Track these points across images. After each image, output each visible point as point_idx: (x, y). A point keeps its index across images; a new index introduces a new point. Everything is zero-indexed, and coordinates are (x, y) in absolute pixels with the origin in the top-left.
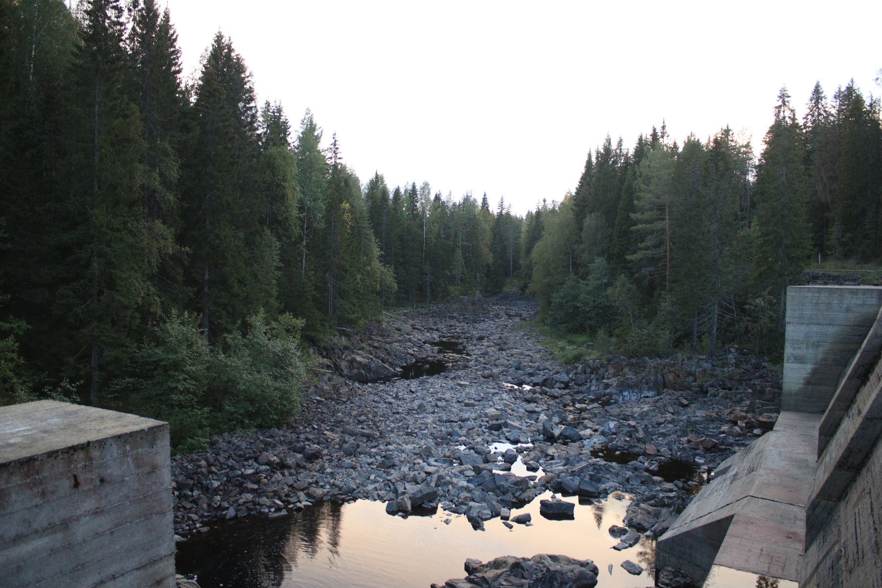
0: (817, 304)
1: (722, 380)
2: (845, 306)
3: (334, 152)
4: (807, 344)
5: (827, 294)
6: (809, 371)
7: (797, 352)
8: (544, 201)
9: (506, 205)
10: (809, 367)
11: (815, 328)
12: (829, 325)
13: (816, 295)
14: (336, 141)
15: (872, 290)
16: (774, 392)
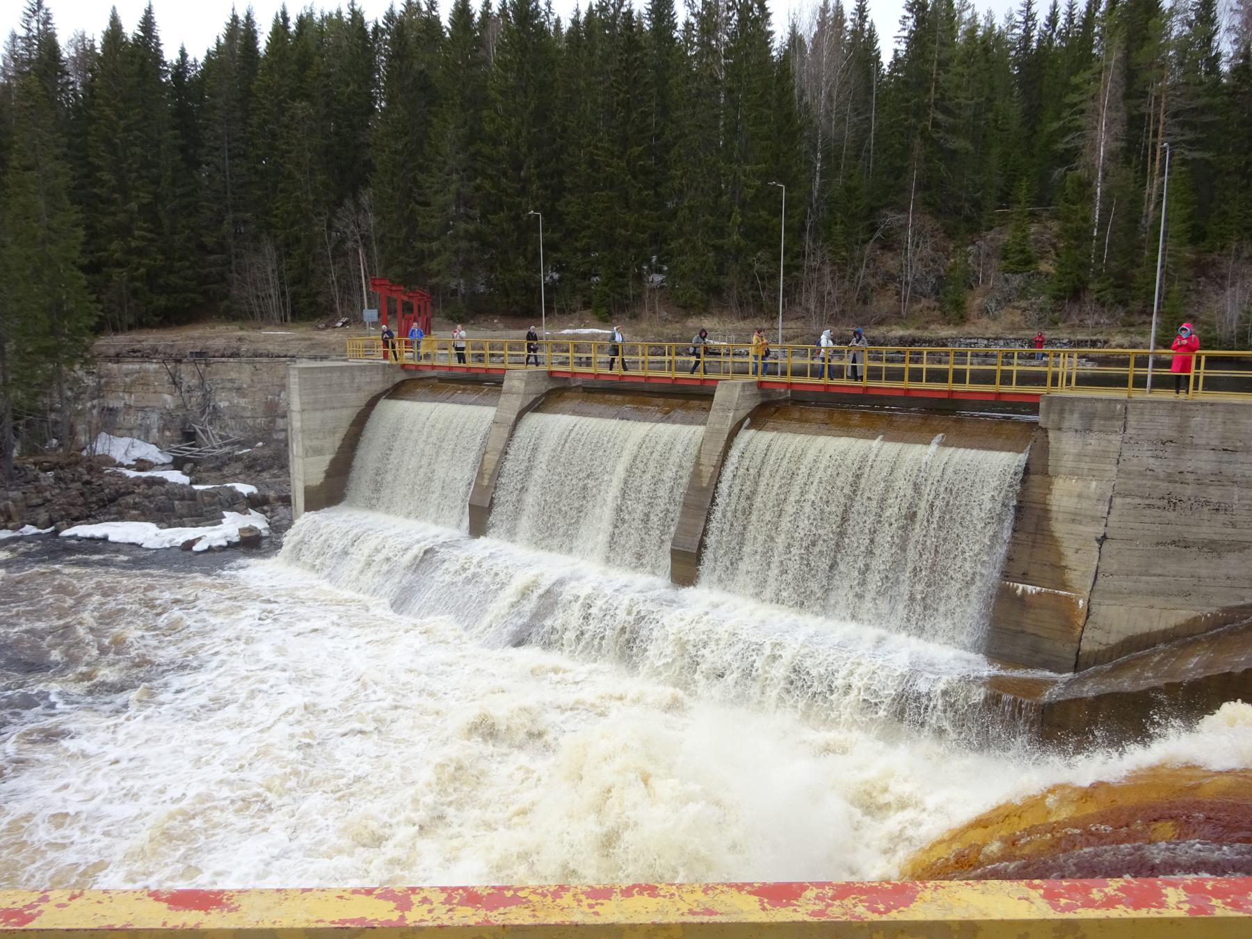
0: (330, 385)
1: (63, 509)
2: (356, 385)
5: (339, 374)
6: (328, 462)
10: (327, 458)
11: (330, 413)
12: (343, 407)
13: (329, 375)
15: (342, 367)
16: (189, 505)
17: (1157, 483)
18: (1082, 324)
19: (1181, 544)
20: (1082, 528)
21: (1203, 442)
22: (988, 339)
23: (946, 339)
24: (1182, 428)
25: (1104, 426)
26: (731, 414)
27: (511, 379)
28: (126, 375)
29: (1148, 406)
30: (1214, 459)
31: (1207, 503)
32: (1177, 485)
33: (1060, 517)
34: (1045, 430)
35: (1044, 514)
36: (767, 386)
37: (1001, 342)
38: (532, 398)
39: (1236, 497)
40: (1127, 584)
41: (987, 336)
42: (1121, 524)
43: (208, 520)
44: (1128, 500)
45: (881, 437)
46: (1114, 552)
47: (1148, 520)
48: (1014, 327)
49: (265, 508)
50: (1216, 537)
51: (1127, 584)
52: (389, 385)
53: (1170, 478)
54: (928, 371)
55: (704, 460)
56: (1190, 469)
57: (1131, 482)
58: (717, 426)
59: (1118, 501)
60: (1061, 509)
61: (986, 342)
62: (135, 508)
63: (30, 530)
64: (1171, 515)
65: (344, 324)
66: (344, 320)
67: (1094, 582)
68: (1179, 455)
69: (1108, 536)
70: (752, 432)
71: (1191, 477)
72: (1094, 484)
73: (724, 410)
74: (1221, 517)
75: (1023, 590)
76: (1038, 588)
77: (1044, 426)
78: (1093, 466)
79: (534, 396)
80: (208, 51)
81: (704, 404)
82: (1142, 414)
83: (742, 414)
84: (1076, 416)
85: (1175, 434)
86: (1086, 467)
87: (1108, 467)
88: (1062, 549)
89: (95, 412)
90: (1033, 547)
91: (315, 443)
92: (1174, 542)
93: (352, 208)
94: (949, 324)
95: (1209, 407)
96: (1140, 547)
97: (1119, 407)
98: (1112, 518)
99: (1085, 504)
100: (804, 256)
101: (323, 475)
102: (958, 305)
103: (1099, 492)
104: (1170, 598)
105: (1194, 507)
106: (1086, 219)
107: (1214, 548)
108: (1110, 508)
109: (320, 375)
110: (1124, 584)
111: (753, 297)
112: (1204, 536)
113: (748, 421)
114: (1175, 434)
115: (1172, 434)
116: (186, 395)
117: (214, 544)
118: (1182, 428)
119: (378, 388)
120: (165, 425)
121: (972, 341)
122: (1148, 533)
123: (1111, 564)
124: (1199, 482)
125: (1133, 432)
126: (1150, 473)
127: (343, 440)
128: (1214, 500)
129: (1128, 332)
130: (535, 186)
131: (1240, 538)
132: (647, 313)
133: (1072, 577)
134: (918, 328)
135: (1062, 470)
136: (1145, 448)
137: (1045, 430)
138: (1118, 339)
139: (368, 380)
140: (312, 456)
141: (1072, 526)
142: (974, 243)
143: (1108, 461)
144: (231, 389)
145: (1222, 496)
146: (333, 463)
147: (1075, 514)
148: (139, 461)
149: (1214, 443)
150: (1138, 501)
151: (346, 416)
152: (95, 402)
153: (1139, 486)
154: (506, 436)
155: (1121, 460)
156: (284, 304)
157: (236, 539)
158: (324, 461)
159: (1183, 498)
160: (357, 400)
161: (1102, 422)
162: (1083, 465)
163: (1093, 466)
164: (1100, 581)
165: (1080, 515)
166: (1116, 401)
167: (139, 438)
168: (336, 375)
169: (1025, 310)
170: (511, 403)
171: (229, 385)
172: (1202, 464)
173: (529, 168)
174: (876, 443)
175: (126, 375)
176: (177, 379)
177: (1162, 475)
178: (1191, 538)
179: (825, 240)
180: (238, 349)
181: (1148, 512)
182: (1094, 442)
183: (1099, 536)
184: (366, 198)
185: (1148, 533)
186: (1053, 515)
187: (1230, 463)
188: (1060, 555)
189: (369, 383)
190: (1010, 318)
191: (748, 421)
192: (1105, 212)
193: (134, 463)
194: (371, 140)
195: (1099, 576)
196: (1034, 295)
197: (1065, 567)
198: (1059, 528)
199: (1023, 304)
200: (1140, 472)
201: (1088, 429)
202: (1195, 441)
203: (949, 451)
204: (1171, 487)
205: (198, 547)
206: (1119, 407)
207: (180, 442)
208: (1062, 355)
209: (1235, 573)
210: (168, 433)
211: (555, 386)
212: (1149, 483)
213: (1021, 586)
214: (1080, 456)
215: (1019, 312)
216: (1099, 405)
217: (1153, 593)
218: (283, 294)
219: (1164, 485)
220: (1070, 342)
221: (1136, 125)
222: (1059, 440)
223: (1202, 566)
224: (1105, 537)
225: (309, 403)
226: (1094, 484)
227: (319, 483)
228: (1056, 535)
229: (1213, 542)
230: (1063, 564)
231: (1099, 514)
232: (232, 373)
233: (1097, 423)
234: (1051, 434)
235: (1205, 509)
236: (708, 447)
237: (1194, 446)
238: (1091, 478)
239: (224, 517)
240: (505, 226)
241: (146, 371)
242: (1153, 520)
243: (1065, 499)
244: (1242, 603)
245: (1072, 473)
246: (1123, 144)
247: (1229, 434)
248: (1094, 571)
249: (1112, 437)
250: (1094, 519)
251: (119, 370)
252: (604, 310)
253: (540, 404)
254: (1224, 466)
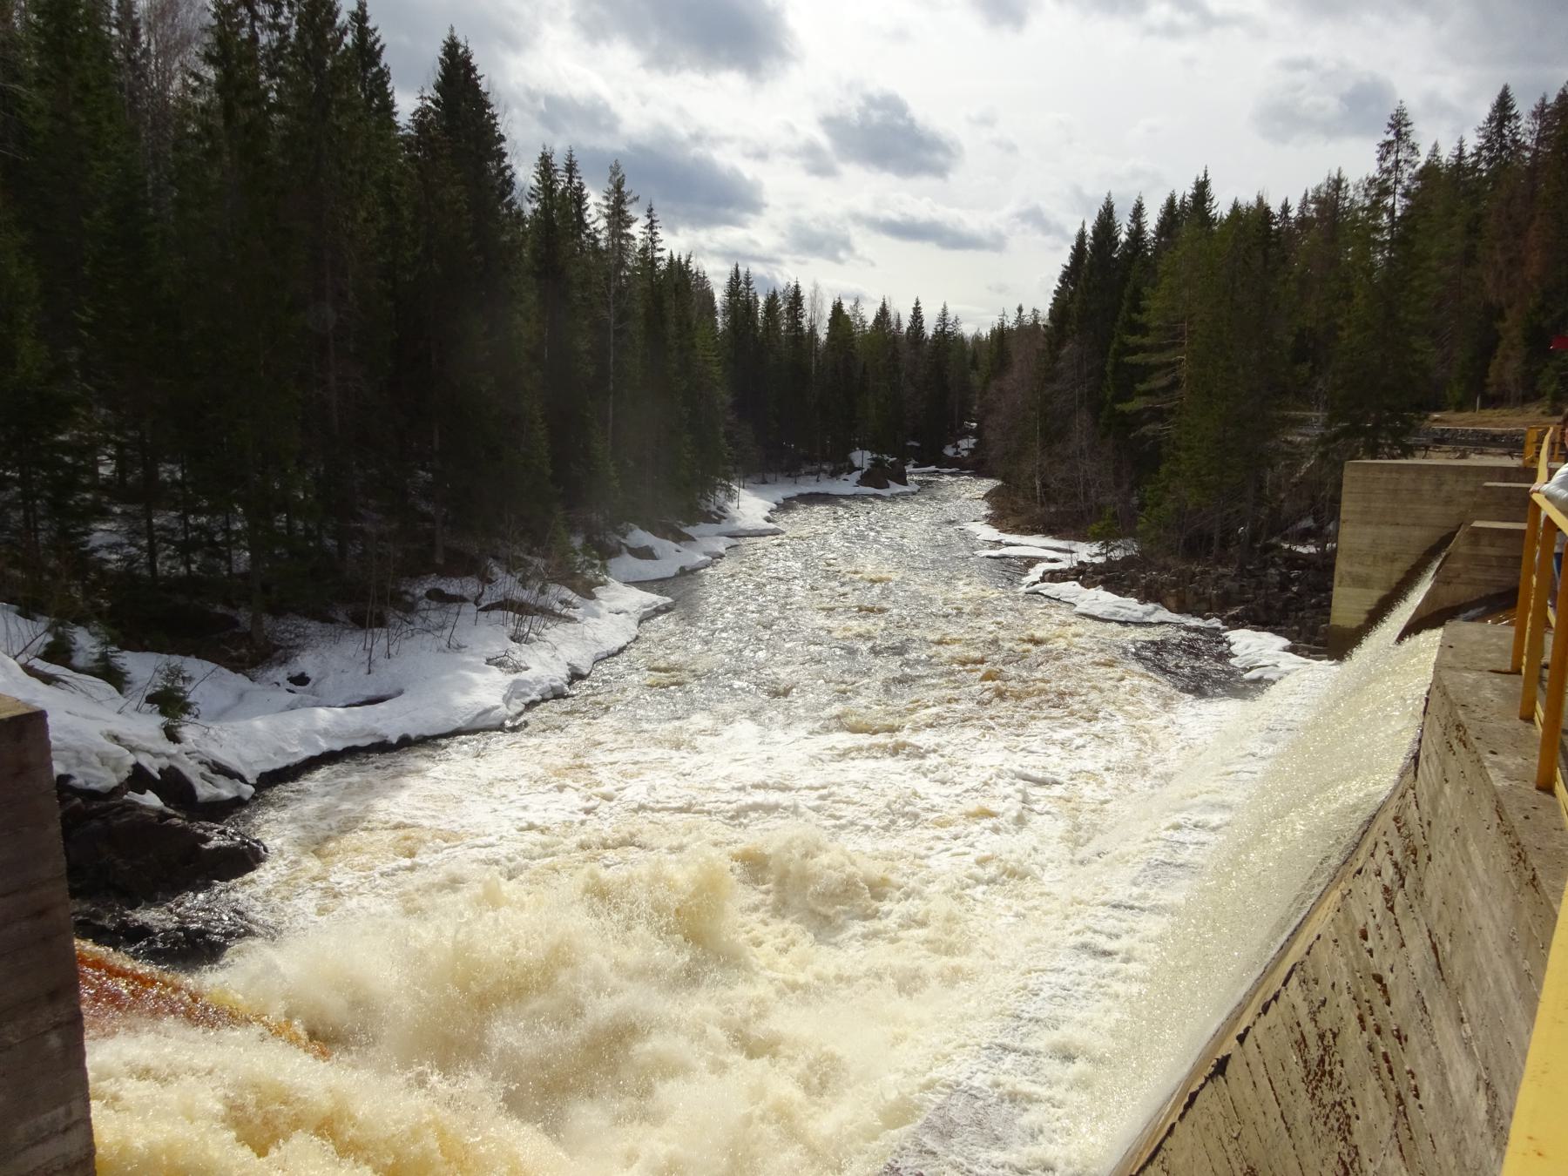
3: (651, 239)
4: (1375, 557)
6: (1375, 600)
7: (1358, 569)
8: (1020, 310)
9: (951, 317)
11: (1389, 531)
12: (1414, 525)
13: (1395, 475)
14: (652, 221)
63: (1215, 623)
101: (1364, 617)
139: (1470, 488)
140: (1349, 586)
191: (1472, 613)
195: (1159, 1158)
227: (1355, 625)
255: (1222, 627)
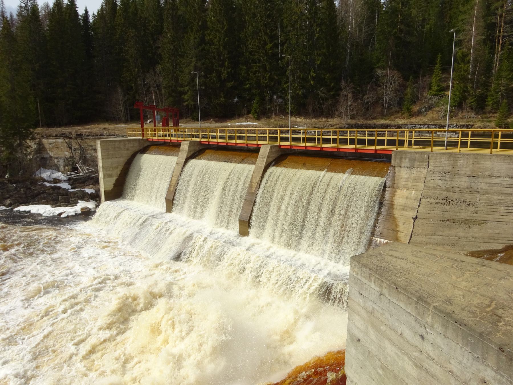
0: (115, 148)
2: (126, 148)
5: (118, 143)
6: (115, 180)
11: (115, 160)
13: (114, 143)
16: (65, 198)
17: (442, 192)
18: (463, 118)
19: (451, 221)
20: (407, 213)
21: (463, 172)
22: (420, 125)
23: (402, 125)
24: (453, 166)
25: (419, 165)
26: (265, 160)
27: (183, 145)
28: (50, 144)
29: (439, 155)
30: (468, 181)
31: (464, 202)
32: (451, 193)
33: (398, 208)
34: (394, 167)
35: (391, 206)
36: (282, 147)
37: (426, 126)
38: (192, 153)
39: (478, 199)
40: (425, 240)
41: (420, 123)
42: (425, 212)
43: (71, 204)
44: (428, 200)
45: (326, 170)
46: (420, 224)
47: (437, 210)
48: (433, 119)
49: (97, 199)
50: (468, 218)
51: (425, 240)
52: (142, 147)
53: (448, 190)
54: (368, 140)
55: (254, 181)
56: (457, 186)
57: (430, 192)
58: (260, 165)
59: (423, 200)
60: (399, 204)
61: (419, 126)
62: (44, 199)
64: (447, 207)
65: (150, 122)
66: (150, 120)
67: (410, 239)
68: (452, 179)
69: (418, 217)
70: (275, 167)
71: (457, 190)
72: (414, 192)
73: (263, 158)
74: (471, 209)
75: (380, 241)
76: (386, 241)
77: (394, 165)
78: (414, 184)
79: (193, 152)
80: (98, 10)
81: (255, 154)
82: (436, 159)
83: (271, 159)
84: (407, 160)
85: (451, 169)
86: (411, 184)
87: (420, 184)
88: (398, 223)
89: (38, 159)
90: (385, 221)
91: (109, 172)
92: (448, 220)
93: (153, 74)
94: (404, 118)
95: (466, 156)
96: (432, 222)
97: (426, 156)
98: (420, 208)
99: (409, 202)
100: (341, 89)
101: (113, 186)
102: (409, 110)
103: (415, 196)
104: (445, 246)
105: (458, 204)
106: (466, 71)
107: (467, 223)
108: (420, 203)
109: (109, 144)
110: (424, 239)
111: (319, 107)
112: (462, 217)
113: (273, 163)
114: (451, 169)
115: (449, 169)
116: (74, 152)
117: (70, 214)
118: (453, 166)
119: (136, 149)
120: (65, 164)
121: (413, 125)
122: (436, 215)
123: (418, 230)
124: (461, 192)
125: (432, 168)
126: (439, 187)
127: (121, 171)
128: (468, 200)
129: (483, 121)
130: (227, 63)
131: (479, 219)
132: (274, 116)
133: (401, 235)
134: (390, 120)
135: (400, 186)
136: (437, 176)
137: (394, 167)
138: (479, 124)
139: (132, 145)
141: (402, 212)
142: (417, 83)
143: (420, 181)
144: (91, 150)
145: (471, 198)
146: (117, 181)
147: (404, 206)
148: (54, 179)
149: (469, 173)
150: (432, 200)
151: (122, 161)
152: (38, 155)
153: (433, 193)
154: (180, 169)
155: (426, 181)
156: (127, 114)
157: (80, 212)
158: (113, 180)
159: (453, 199)
160: (129, 154)
161: (418, 163)
162: (410, 184)
163: (414, 184)
164: (413, 238)
165: (406, 207)
166: (424, 153)
167: (55, 170)
168: (117, 144)
169: (438, 111)
170: (183, 155)
171: (90, 148)
172: (462, 183)
173: (224, 55)
174: (323, 173)
175: (50, 144)
176: (70, 146)
177: (444, 188)
178: (456, 218)
179: (350, 83)
180: (103, 133)
181: (437, 206)
182: (415, 172)
183: (414, 217)
184: (159, 68)
185: (436, 215)
186: (395, 207)
187: (475, 183)
188: (397, 225)
189: (133, 147)
190: (431, 115)
191: (273, 163)
192: (475, 67)
193: (53, 180)
194: (160, 45)
196: (443, 105)
197: (398, 231)
198: (397, 213)
199: (437, 109)
200: (434, 187)
201: (412, 167)
202: (460, 172)
203: (353, 176)
204: (448, 194)
205: (63, 216)
206: (426, 156)
207: (72, 171)
208: (406, 131)
209: (477, 235)
210: (67, 168)
211: (203, 148)
212: (438, 192)
213: (379, 239)
214: (408, 179)
215: (435, 112)
216: (417, 155)
217: (437, 244)
218: (127, 109)
219: (444, 193)
220: (457, 125)
221: (491, 27)
222: (400, 172)
223: (461, 232)
224: (416, 217)
225: (105, 156)
226: (414, 192)
227: (111, 189)
228: (396, 216)
229: (466, 220)
230: (398, 229)
231: (415, 207)
232: (92, 143)
233: (416, 164)
234: (396, 169)
235: (463, 204)
236: (255, 174)
237: (459, 175)
238: (412, 189)
239: (78, 203)
240: (215, 79)
241: (58, 142)
242: (439, 209)
243: (401, 199)
244: (479, 249)
245: (404, 187)
246: (483, 37)
247: (475, 169)
248: (411, 233)
249: (422, 170)
250: (413, 209)
251: (47, 142)
252: (256, 114)
253: (194, 155)
254: (473, 184)
255: (8, 208)
